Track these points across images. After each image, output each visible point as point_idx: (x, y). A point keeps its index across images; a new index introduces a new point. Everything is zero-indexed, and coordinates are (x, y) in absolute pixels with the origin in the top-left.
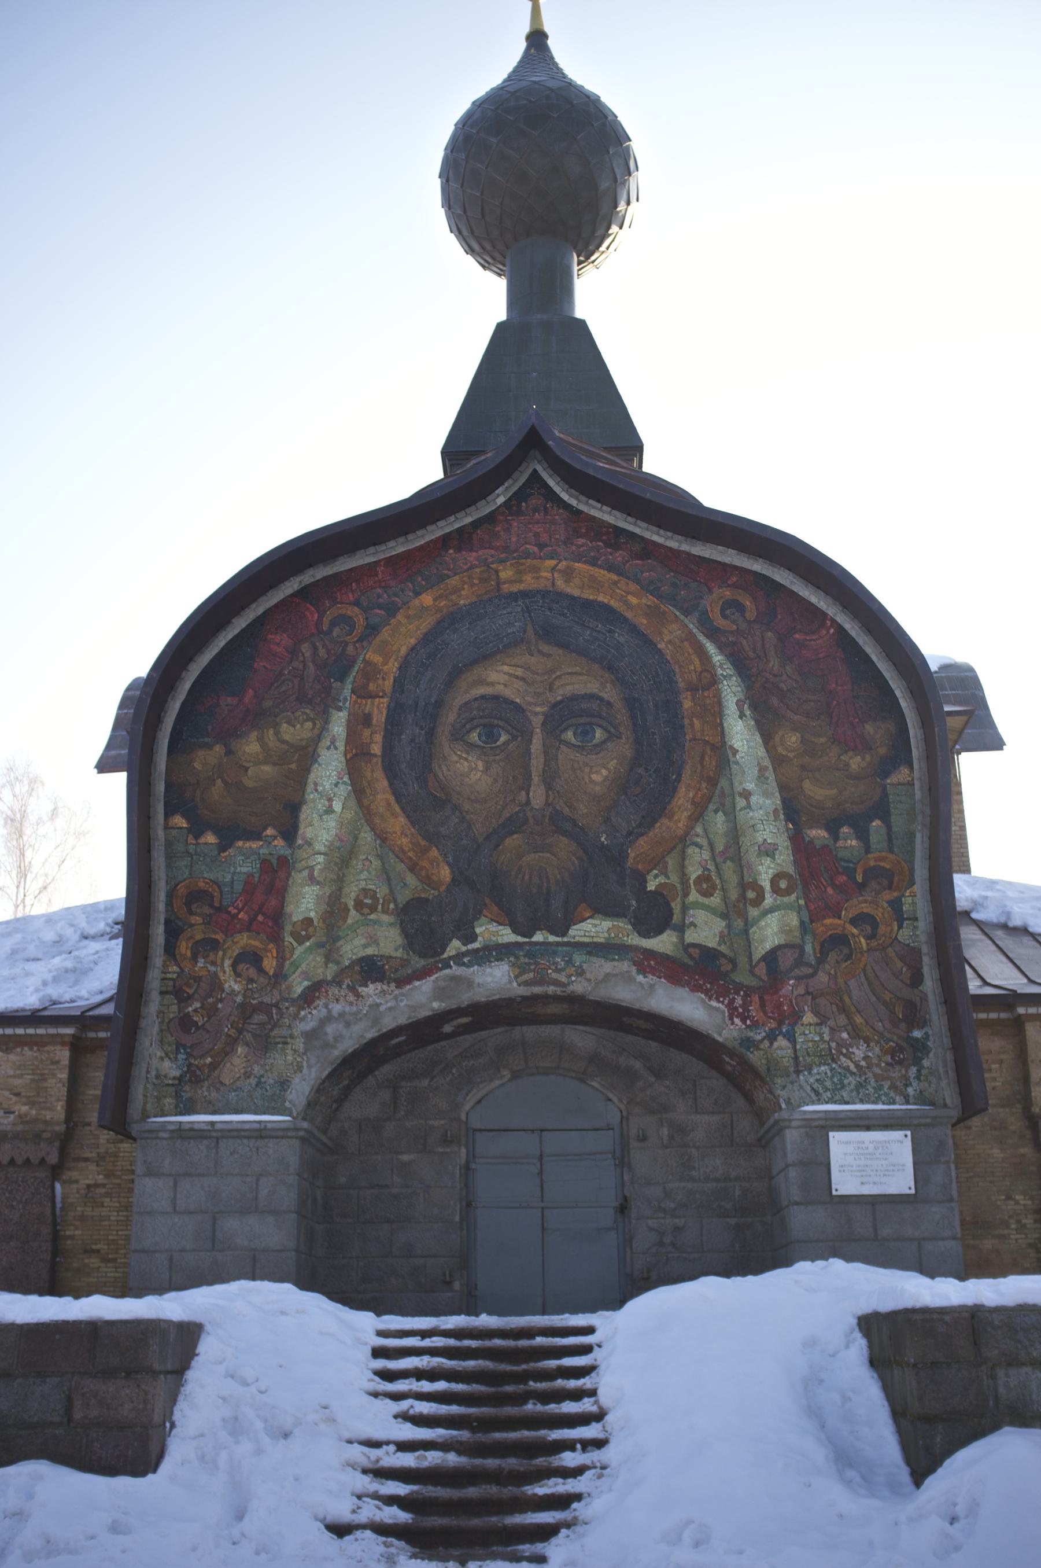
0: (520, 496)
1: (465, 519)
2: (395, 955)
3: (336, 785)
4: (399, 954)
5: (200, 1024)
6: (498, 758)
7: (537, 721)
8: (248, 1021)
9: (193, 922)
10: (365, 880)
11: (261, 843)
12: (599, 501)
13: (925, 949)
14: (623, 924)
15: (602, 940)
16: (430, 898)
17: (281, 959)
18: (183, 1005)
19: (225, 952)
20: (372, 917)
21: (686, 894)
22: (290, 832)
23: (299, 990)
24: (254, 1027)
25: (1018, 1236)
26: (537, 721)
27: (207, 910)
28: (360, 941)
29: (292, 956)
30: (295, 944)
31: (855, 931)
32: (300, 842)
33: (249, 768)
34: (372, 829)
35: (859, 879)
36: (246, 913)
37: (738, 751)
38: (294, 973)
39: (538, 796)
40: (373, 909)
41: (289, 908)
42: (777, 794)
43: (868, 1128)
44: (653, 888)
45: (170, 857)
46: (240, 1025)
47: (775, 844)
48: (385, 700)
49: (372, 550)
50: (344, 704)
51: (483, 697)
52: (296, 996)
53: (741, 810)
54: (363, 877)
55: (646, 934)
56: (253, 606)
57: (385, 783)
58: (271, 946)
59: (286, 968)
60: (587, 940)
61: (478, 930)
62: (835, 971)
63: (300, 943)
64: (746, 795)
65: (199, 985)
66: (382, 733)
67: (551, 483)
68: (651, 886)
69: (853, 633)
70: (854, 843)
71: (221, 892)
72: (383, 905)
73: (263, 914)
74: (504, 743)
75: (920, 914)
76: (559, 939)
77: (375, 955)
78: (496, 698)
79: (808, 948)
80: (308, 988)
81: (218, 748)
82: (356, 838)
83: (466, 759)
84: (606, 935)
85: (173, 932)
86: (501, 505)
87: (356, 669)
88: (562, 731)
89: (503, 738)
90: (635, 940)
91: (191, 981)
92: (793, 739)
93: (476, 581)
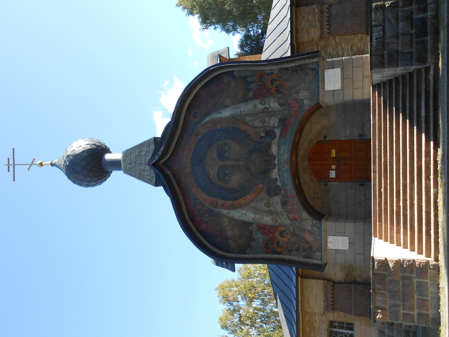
0: (168, 167)
1: (174, 181)
2: (281, 198)
3: (239, 212)
4: (280, 197)
5: (298, 246)
6: (232, 173)
7: (223, 163)
10: (262, 205)
11: (253, 231)
12: (169, 148)
13: (279, 67)
14: (273, 142)
15: (277, 147)
16: (267, 189)
17: (281, 226)
19: (280, 240)
20: (271, 203)
23: (289, 222)
25: (352, 42)
27: (270, 244)
29: (281, 223)
30: (278, 222)
31: (275, 84)
32: (253, 221)
33: (235, 234)
34: (249, 203)
35: (262, 83)
37: (230, 114)
38: (285, 223)
39: (241, 163)
40: (269, 203)
41: (269, 224)
42: (241, 104)
43: (324, 81)
44: (264, 134)
45: (256, 253)
47: (253, 105)
48: (218, 200)
49: (182, 204)
50: (219, 210)
51: (217, 176)
52: (291, 222)
53: (245, 113)
54: (261, 206)
55: (275, 136)
56: (195, 233)
57: (238, 201)
58: (278, 228)
60: (277, 151)
61: (275, 177)
62: (285, 89)
63: (278, 221)
64: (241, 112)
66: (226, 201)
67: (165, 160)
68: (264, 135)
69: (201, 86)
70: (253, 85)
72: (268, 201)
73: (271, 230)
74: (228, 171)
75: (270, 68)
76: (277, 158)
77: (281, 203)
78: (217, 173)
79: (279, 96)
80: (289, 219)
81: (230, 241)
82: (252, 207)
83: (232, 181)
84: (276, 146)
85: (275, 253)
86: (170, 172)
88: (226, 157)
89: (227, 171)
92: (227, 100)
93: (189, 178)
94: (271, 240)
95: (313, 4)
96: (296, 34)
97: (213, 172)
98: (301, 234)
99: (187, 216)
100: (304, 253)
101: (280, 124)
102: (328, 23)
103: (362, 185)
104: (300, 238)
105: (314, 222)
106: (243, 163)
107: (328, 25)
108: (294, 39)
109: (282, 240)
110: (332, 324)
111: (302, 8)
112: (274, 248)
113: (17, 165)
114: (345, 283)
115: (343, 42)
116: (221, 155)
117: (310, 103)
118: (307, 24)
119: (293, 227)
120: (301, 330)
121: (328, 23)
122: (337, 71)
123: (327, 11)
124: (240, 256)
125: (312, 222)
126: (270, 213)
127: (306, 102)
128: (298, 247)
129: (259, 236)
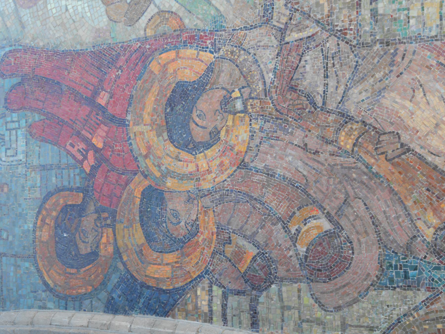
5: (327, 226)
8: (319, 100)
9: (111, 249)
18: (281, 272)
24: (332, 83)
30: (152, 10)
36: (93, 131)
46: (332, 118)
58: (154, 67)
59: (201, 25)
65: (240, 232)
71: (59, 190)
73: (96, 93)
91: (229, 250)
94: (100, 179)
109: (182, 177)
112: (118, 252)
119: (283, 32)
128: (329, 235)
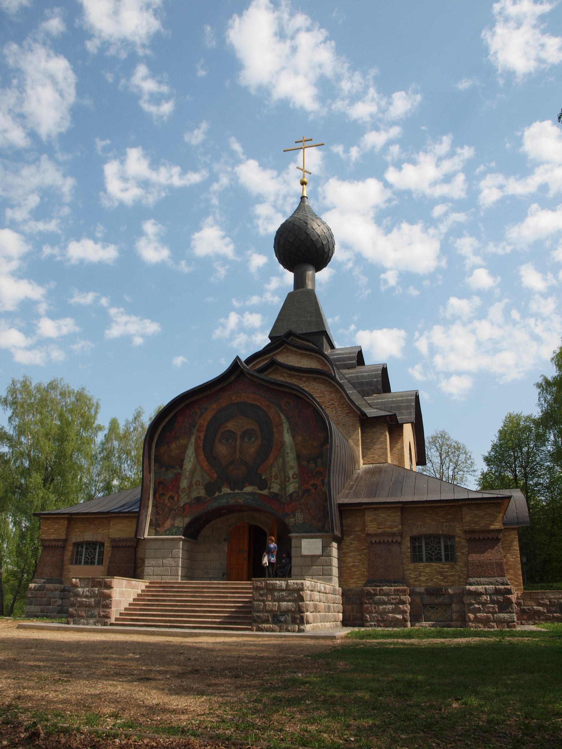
4: (204, 496)
7: (238, 437)
14: (256, 488)
20: (199, 487)
21: (271, 479)
22: (181, 466)
26: (238, 437)
28: (196, 493)
31: (312, 488)
32: (183, 469)
35: (314, 474)
39: (238, 456)
40: (199, 485)
41: (181, 485)
43: (312, 538)
45: (155, 473)
55: (261, 490)
57: (202, 454)
58: (176, 495)
61: (222, 490)
64: (288, 453)
68: (263, 478)
70: (313, 465)
79: (300, 493)
81: (166, 446)
87: (197, 425)
89: (230, 441)
90: (259, 491)
92: (300, 438)
95: (402, 524)
96: (373, 508)
97: (230, 426)
98: (170, 516)
99: (190, 400)
100: (154, 519)
101: (273, 494)
102: (382, 541)
103: (223, 575)
104: (167, 515)
105: (181, 529)
106: (237, 457)
107: (380, 541)
108: (367, 507)
110: (102, 544)
111: (399, 514)
113: (304, 152)
114: (135, 558)
115: (362, 557)
116: (247, 434)
117: (291, 525)
118: (383, 520)
120: (96, 516)
121: (382, 541)
122: (319, 552)
123: (394, 541)
124: (153, 457)
125: (180, 527)
126: (190, 486)
127: (292, 520)
129: (170, 475)
